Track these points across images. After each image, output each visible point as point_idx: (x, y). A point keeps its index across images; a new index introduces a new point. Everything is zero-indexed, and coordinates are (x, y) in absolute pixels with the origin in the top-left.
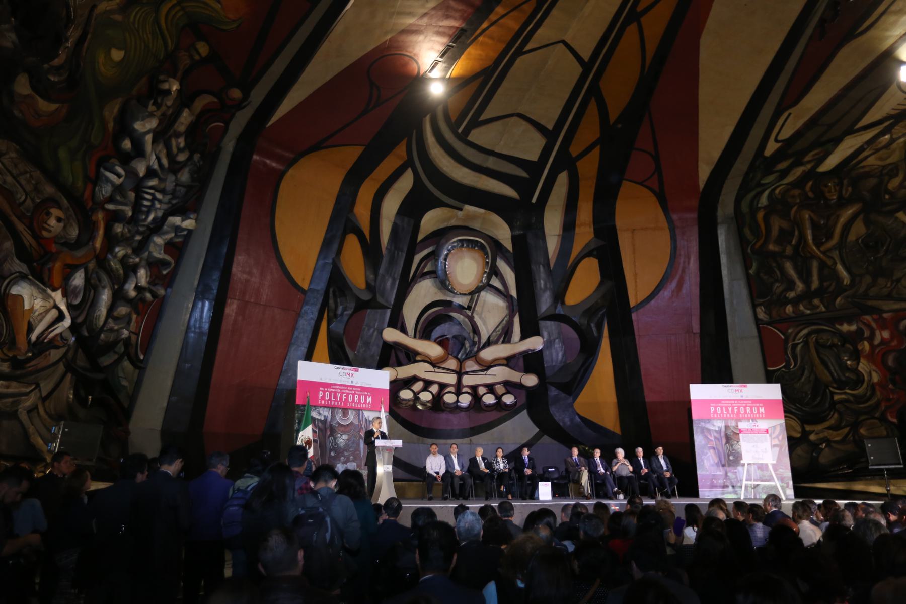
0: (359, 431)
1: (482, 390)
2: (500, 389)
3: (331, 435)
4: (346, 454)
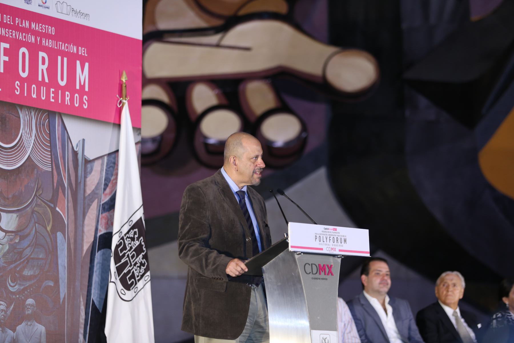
0: (54, 200)
1: (202, 97)
2: (259, 97)
4: (14, 288)
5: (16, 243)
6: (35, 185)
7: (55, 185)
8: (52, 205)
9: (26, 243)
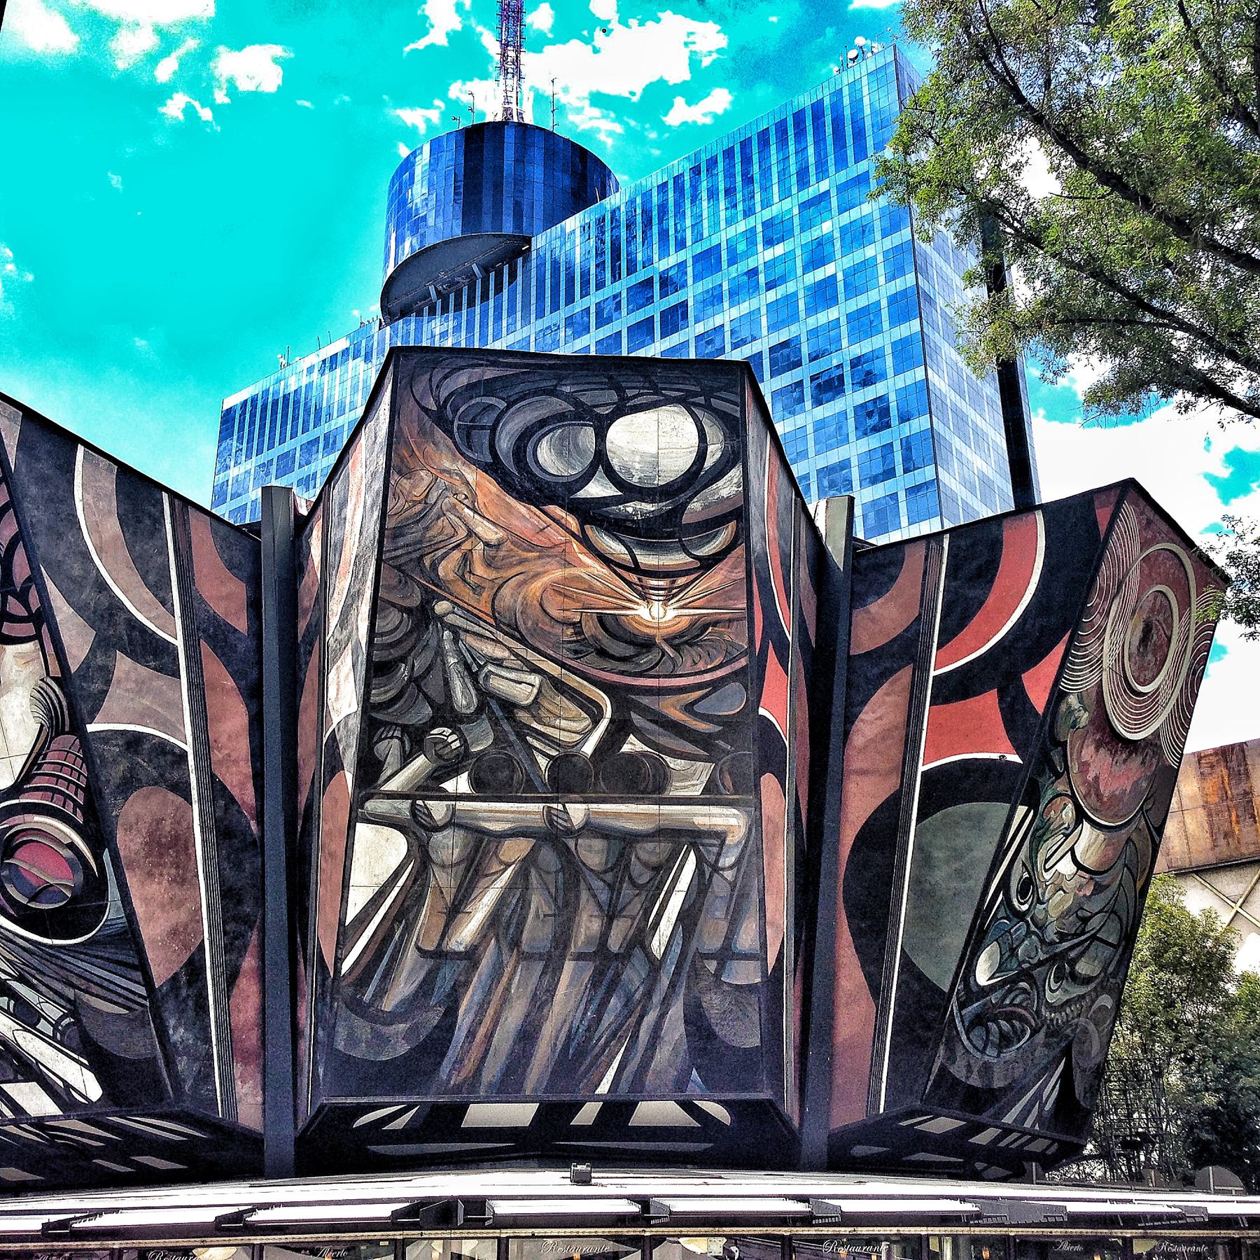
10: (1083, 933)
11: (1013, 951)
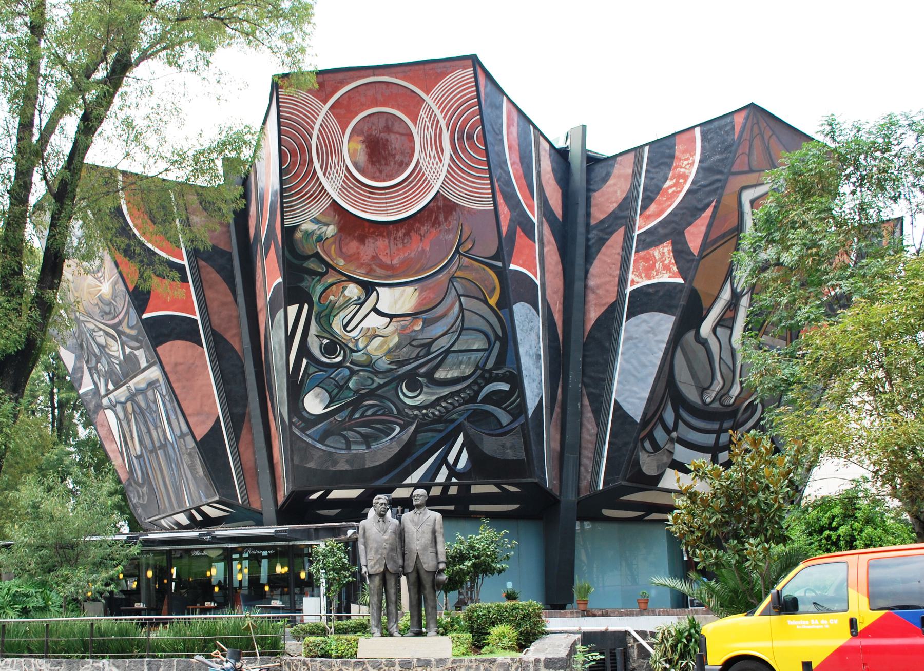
0: (503, 253)
3: (294, 292)
5: (415, 331)
6: (455, 238)
7: (504, 229)
8: (500, 264)
9: (438, 329)
10: (428, 353)
11: (342, 387)
